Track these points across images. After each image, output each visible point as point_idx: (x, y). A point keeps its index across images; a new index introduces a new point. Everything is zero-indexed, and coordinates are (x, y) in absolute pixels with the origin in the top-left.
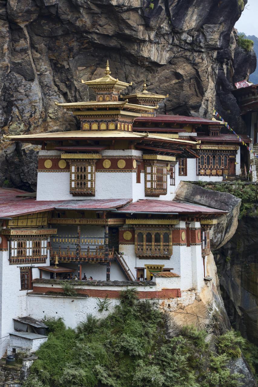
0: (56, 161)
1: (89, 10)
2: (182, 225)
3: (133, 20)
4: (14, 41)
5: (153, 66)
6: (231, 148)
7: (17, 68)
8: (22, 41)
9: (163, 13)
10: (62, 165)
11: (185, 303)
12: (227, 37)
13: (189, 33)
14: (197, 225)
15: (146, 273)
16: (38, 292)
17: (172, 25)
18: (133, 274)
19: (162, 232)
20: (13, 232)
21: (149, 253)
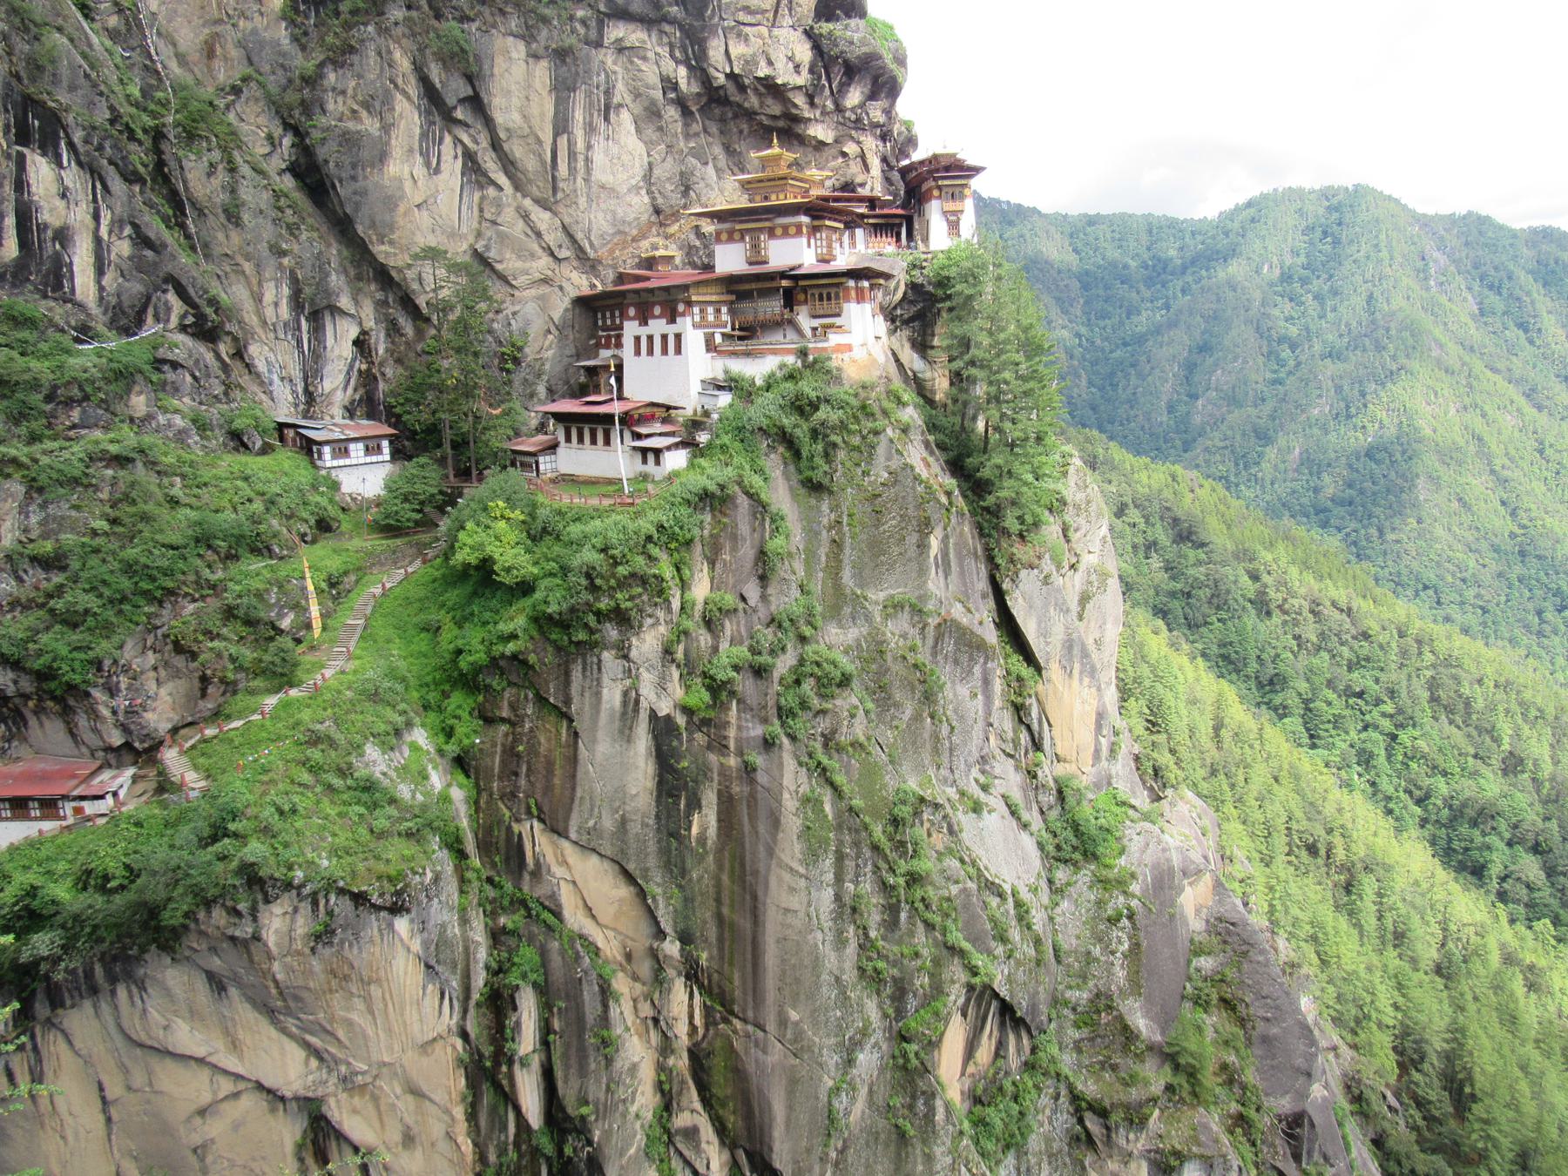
0: (731, 233)
1: (756, 89)
2: (851, 283)
3: (800, 100)
4: (686, 125)
5: (820, 145)
6: (897, 221)
10: (737, 236)
12: (888, 112)
13: (853, 109)
14: (866, 284)
16: (720, 353)
18: (808, 333)
19: (833, 291)
20: (694, 298)
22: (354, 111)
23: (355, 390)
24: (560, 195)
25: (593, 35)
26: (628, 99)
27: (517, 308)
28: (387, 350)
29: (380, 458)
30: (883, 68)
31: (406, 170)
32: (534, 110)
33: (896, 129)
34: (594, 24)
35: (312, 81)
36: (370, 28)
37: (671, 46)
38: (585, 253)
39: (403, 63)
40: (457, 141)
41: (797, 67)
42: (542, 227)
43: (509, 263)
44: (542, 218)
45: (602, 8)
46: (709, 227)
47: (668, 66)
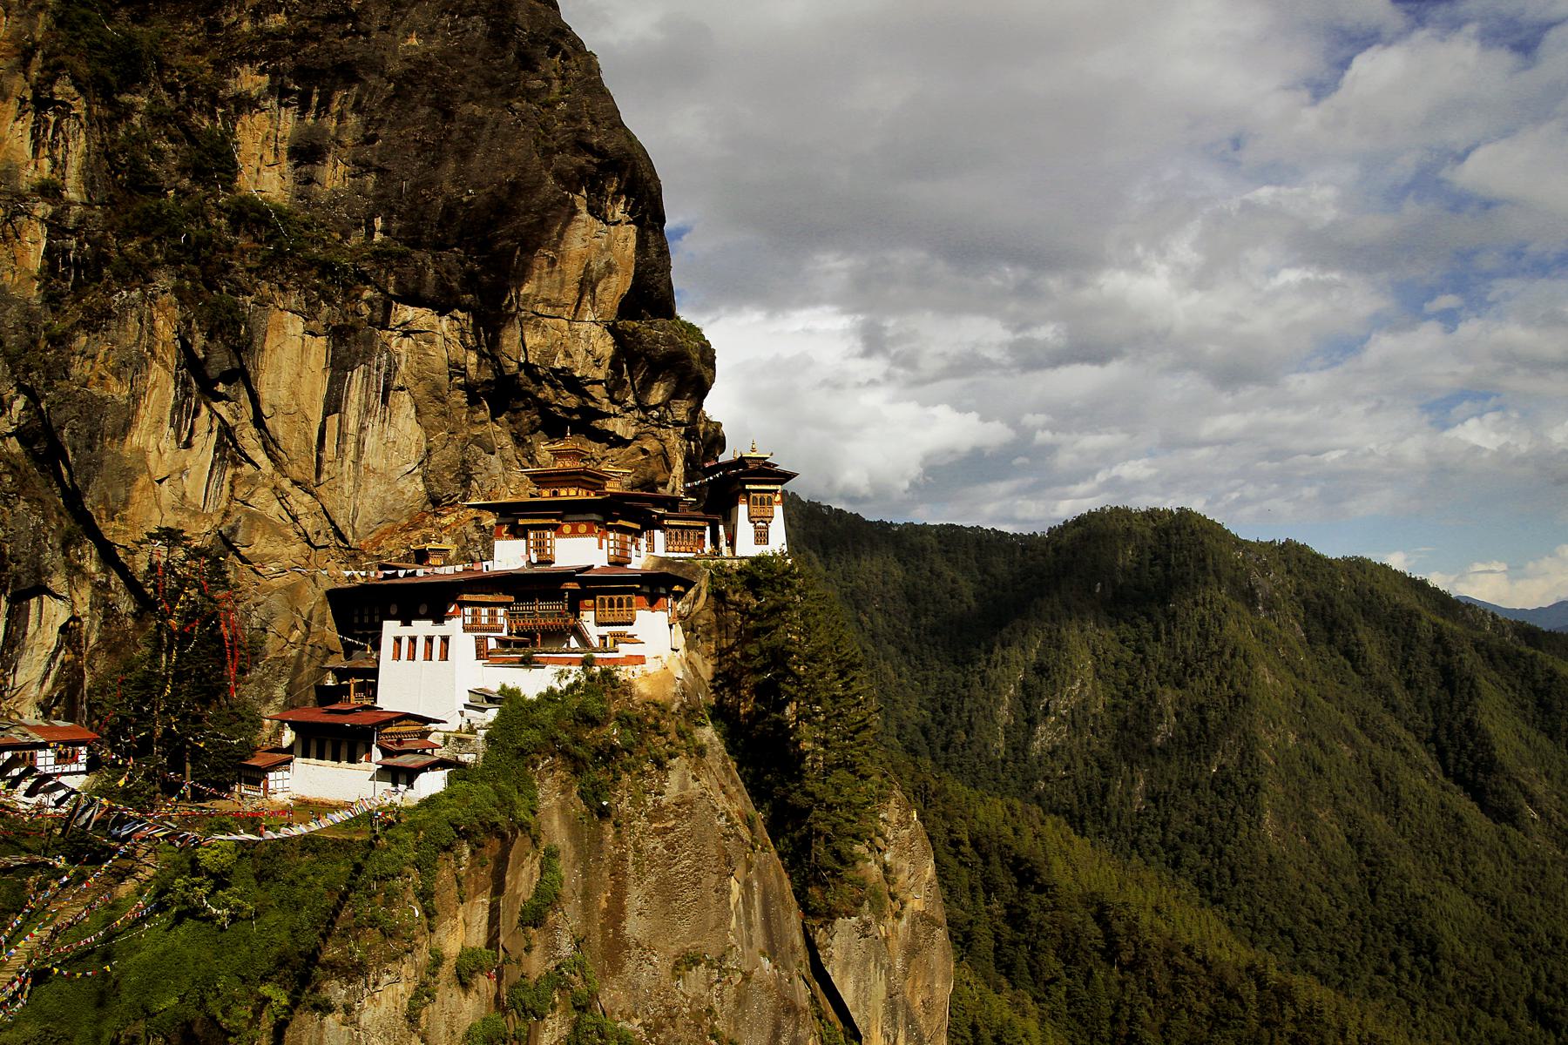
3: (598, 391)
5: (620, 442)
6: (701, 524)
7: (477, 440)
8: (482, 413)
9: (628, 387)
11: (650, 671)
13: (655, 407)
15: (610, 641)
17: (636, 398)
19: (624, 597)
20: (466, 597)
21: (611, 620)
22: (102, 378)
23: (54, 685)
24: (324, 477)
25: (378, 316)
26: (411, 382)
27: (261, 598)
28: (100, 640)
29: (74, 768)
30: (690, 367)
31: (152, 442)
32: (306, 389)
33: (702, 426)
34: (379, 305)
35: (60, 341)
36: (136, 294)
37: (463, 332)
38: (346, 542)
39: (165, 330)
40: (214, 414)
41: (597, 362)
42: (300, 510)
43: (260, 545)
44: (301, 502)
45: (391, 290)
46: (490, 520)
47: (458, 352)
